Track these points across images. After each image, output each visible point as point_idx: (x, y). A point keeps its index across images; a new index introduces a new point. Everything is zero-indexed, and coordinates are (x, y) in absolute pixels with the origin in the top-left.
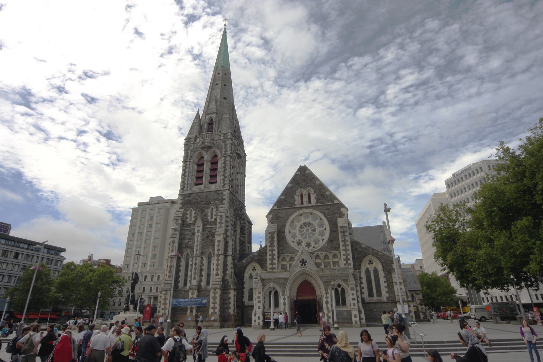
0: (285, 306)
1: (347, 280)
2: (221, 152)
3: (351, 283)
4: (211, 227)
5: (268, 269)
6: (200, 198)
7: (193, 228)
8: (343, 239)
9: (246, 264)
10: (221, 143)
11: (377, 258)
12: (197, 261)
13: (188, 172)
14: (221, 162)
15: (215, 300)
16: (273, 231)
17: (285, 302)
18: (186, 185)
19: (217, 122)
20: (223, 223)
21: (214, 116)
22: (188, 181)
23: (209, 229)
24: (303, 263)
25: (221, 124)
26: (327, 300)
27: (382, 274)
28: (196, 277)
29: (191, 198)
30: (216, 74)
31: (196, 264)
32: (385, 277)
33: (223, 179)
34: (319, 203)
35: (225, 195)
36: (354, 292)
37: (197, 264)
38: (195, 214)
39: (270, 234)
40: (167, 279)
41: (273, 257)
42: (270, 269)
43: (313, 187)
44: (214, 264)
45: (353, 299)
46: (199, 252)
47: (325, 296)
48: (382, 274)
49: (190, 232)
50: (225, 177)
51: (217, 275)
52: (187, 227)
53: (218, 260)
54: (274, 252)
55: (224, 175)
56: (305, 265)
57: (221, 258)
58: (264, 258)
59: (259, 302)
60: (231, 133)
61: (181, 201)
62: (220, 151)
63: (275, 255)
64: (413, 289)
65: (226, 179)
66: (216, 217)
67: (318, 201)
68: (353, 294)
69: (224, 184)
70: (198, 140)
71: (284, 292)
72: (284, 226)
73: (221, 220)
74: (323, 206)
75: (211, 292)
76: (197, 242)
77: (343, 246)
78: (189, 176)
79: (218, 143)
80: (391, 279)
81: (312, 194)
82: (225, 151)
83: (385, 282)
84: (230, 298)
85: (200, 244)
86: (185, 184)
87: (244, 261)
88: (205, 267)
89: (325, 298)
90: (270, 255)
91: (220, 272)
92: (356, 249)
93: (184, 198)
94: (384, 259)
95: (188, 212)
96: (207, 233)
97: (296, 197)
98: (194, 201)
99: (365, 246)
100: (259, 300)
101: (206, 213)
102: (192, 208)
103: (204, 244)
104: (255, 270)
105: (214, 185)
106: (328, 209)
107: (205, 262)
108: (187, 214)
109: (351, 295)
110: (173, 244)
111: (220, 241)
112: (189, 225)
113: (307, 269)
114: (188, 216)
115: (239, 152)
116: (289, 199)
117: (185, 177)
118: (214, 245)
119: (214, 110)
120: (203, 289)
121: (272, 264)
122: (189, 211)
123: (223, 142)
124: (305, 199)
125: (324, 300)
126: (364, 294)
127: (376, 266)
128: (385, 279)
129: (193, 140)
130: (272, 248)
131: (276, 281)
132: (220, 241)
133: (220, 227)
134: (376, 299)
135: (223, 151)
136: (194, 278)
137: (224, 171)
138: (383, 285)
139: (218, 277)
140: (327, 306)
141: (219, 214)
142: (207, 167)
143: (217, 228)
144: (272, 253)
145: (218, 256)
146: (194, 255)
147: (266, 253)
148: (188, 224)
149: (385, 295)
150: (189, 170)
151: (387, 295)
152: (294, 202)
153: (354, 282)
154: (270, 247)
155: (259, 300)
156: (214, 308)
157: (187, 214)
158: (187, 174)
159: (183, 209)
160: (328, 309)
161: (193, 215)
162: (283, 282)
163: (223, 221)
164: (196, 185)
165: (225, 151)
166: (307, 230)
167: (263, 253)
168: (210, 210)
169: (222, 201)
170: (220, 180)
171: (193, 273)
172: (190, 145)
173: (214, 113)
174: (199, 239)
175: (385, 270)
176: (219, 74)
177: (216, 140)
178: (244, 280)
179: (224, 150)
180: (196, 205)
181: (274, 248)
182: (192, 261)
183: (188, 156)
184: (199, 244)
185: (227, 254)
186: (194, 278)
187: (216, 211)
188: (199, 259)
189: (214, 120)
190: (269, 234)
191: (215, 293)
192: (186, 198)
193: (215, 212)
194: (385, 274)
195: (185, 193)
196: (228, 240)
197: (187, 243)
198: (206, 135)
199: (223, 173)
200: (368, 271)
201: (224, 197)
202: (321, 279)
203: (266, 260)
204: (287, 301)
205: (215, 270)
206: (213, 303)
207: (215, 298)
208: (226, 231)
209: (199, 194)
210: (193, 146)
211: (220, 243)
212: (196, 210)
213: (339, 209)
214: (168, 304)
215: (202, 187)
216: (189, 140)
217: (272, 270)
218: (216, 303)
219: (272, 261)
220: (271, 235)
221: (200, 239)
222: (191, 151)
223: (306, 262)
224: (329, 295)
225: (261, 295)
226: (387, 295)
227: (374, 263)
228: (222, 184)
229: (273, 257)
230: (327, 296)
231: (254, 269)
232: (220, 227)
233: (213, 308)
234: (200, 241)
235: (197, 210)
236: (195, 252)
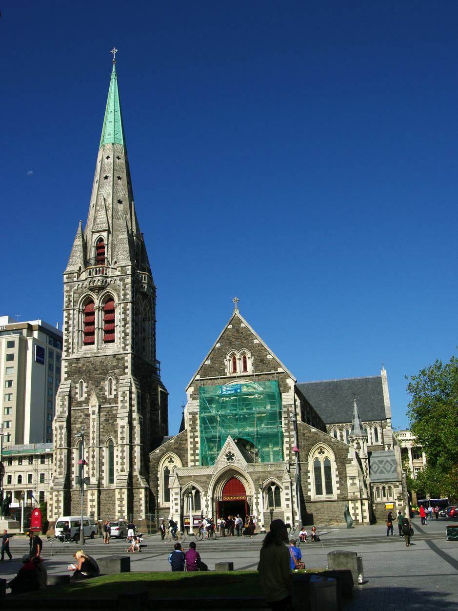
0: (208, 508)
1: (282, 477)
2: (119, 295)
3: (285, 481)
4: (110, 406)
5: (189, 461)
6: (92, 364)
7: (85, 408)
8: (287, 422)
9: (159, 455)
10: (118, 282)
11: (330, 446)
12: (95, 453)
13: (72, 325)
14: (119, 311)
15: (121, 502)
16: (195, 411)
18: (71, 346)
19: (110, 245)
20: (126, 402)
21: (105, 234)
22: (73, 340)
23: (109, 409)
24: (230, 457)
25: (117, 250)
26: (257, 501)
27: (334, 466)
28: (95, 473)
29: (80, 365)
30: (105, 157)
31: (93, 457)
32: (337, 470)
33: (123, 338)
34: (258, 370)
35: (127, 361)
36: (289, 491)
37: (95, 456)
38: (87, 387)
39: (191, 416)
40: (58, 476)
41: (195, 446)
42: (192, 461)
43: (250, 349)
44: (117, 456)
45: (287, 500)
46: (97, 441)
47: (255, 496)
48: (334, 466)
49: (82, 414)
50: (126, 335)
51: (122, 471)
52: (77, 406)
53: (123, 451)
54: (196, 440)
55: (124, 332)
56: (232, 459)
57: (127, 448)
58: (183, 446)
59: (176, 504)
60: (131, 265)
61: (66, 370)
62: (118, 294)
63: (198, 443)
65: (128, 337)
66: (117, 393)
67: (256, 369)
68: (287, 494)
69: (126, 345)
70: (84, 276)
71: (206, 492)
73: (124, 398)
74: (263, 376)
75: (117, 491)
76: (93, 427)
78: (73, 332)
79: (113, 282)
80: (344, 473)
81: (248, 358)
82: (125, 295)
83: (337, 476)
84: (141, 499)
85: (97, 430)
86: (70, 344)
87: (158, 451)
88: (106, 460)
89: (255, 498)
90: (191, 443)
91: (127, 467)
92: (304, 434)
93: (70, 364)
94: (337, 446)
95: (78, 385)
96: (106, 415)
97: (226, 363)
98: (84, 369)
99: (315, 430)
100: (176, 502)
101: (102, 387)
102: (81, 380)
103: (102, 430)
104: (173, 462)
105: (110, 345)
107: (106, 453)
108: (76, 388)
109: (285, 494)
110: (61, 431)
111: (124, 426)
112: (80, 404)
113: (234, 465)
114: (77, 391)
116: (217, 365)
117: (68, 333)
118: (116, 432)
119: (105, 226)
120: (106, 488)
121: (193, 455)
122: (78, 383)
123: (120, 280)
124: (240, 364)
125: (254, 501)
126: (310, 491)
127: (327, 456)
128: (337, 472)
129: (76, 275)
130: (194, 434)
131: (197, 478)
132: (124, 426)
133: (123, 407)
134: (325, 496)
135: (121, 295)
136: (93, 475)
137: (124, 326)
138: (334, 479)
139: (123, 473)
140: (257, 508)
141: (120, 389)
142: (99, 318)
143: (119, 408)
144: (194, 440)
145: (123, 446)
146: (91, 445)
147: (187, 440)
148: (78, 402)
149: (336, 492)
150: (73, 323)
151: (339, 492)
152: (224, 369)
153: (289, 480)
154: (191, 432)
155: (176, 502)
156: (121, 512)
157: (76, 388)
158: (71, 329)
159: (70, 381)
160: (258, 511)
161: (85, 390)
162: (204, 481)
163: (127, 398)
164: (86, 344)
165: (125, 295)
167: (183, 441)
168: (107, 383)
169: (124, 370)
170: (120, 338)
171: (91, 469)
172: (72, 283)
173: (104, 231)
174: (95, 423)
175: (338, 461)
176: (108, 158)
177: (111, 277)
178: (158, 476)
179: (122, 292)
180: (88, 376)
181: (196, 434)
182: (88, 452)
183: (71, 301)
184: (95, 430)
185: (134, 443)
186: (93, 475)
187: (116, 384)
188: (97, 450)
189: (105, 242)
190: (189, 414)
191: (121, 493)
192: (73, 365)
193: (115, 385)
194: (338, 466)
195: (72, 356)
196: (134, 425)
197: (79, 428)
198: (94, 269)
199: (123, 329)
200: (317, 462)
201: (126, 364)
202: (251, 476)
203: (187, 450)
204: (210, 503)
205: (119, 464)
206: (119, 506)
207: (121, 499)
208: (131, 412)
209: (91, 359)
210: (77, 286)
211: (124, 430)
212: (88, 382)
213: (284, 380)
214: (62, 507)
215: (94, 346)
216: (71, 276)
217: (195, 463)
218: (124, 506)
219: (194, 451)
220: (192, 416)
221: (97, 424)
222: (74, 293)
223: (233, 455)
225: (178, 497)
226: (339, 492)
227: (326, 452)
228: (123, 345)
229: (195, 446)
231: (171, 461)
232: (123, 407)
233: (119, 512)
234: (97, 427)
235: (90, 382)
236: (91, 441)
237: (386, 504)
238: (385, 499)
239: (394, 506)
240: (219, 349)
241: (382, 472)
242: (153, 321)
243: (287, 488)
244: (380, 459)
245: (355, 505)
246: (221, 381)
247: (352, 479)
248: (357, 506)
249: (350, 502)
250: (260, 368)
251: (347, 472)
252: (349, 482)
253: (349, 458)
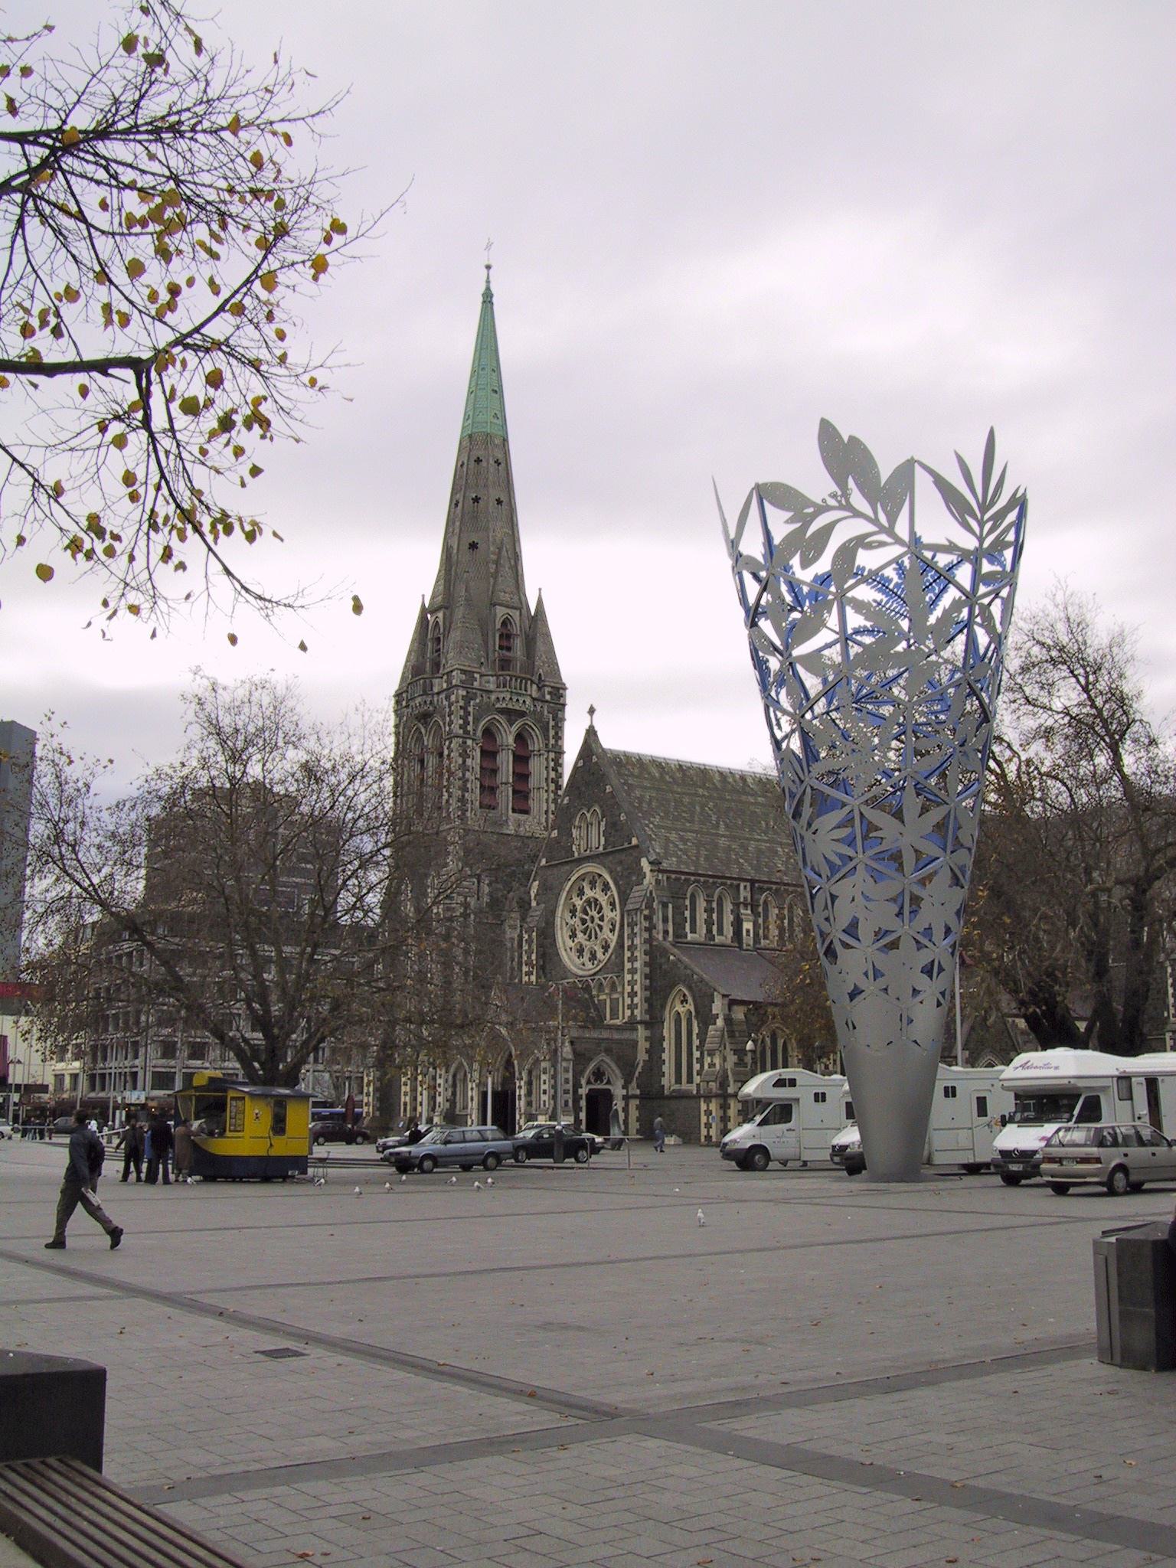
27: (696, 1030)
33: (447, 801)
48: (696, 1030)
50: (450, 796)
72: (553, 912)
77: (629, 960)
106: (621, 862)
115: (504, 705)
165: (450, 726)
166: (592, 918)
240: (568, 806)
242: (552, 755)
246: (567, 867)
249: (702, 1100)
250: (612, 839)
252: (707, 1060)
253: (714, 1012)
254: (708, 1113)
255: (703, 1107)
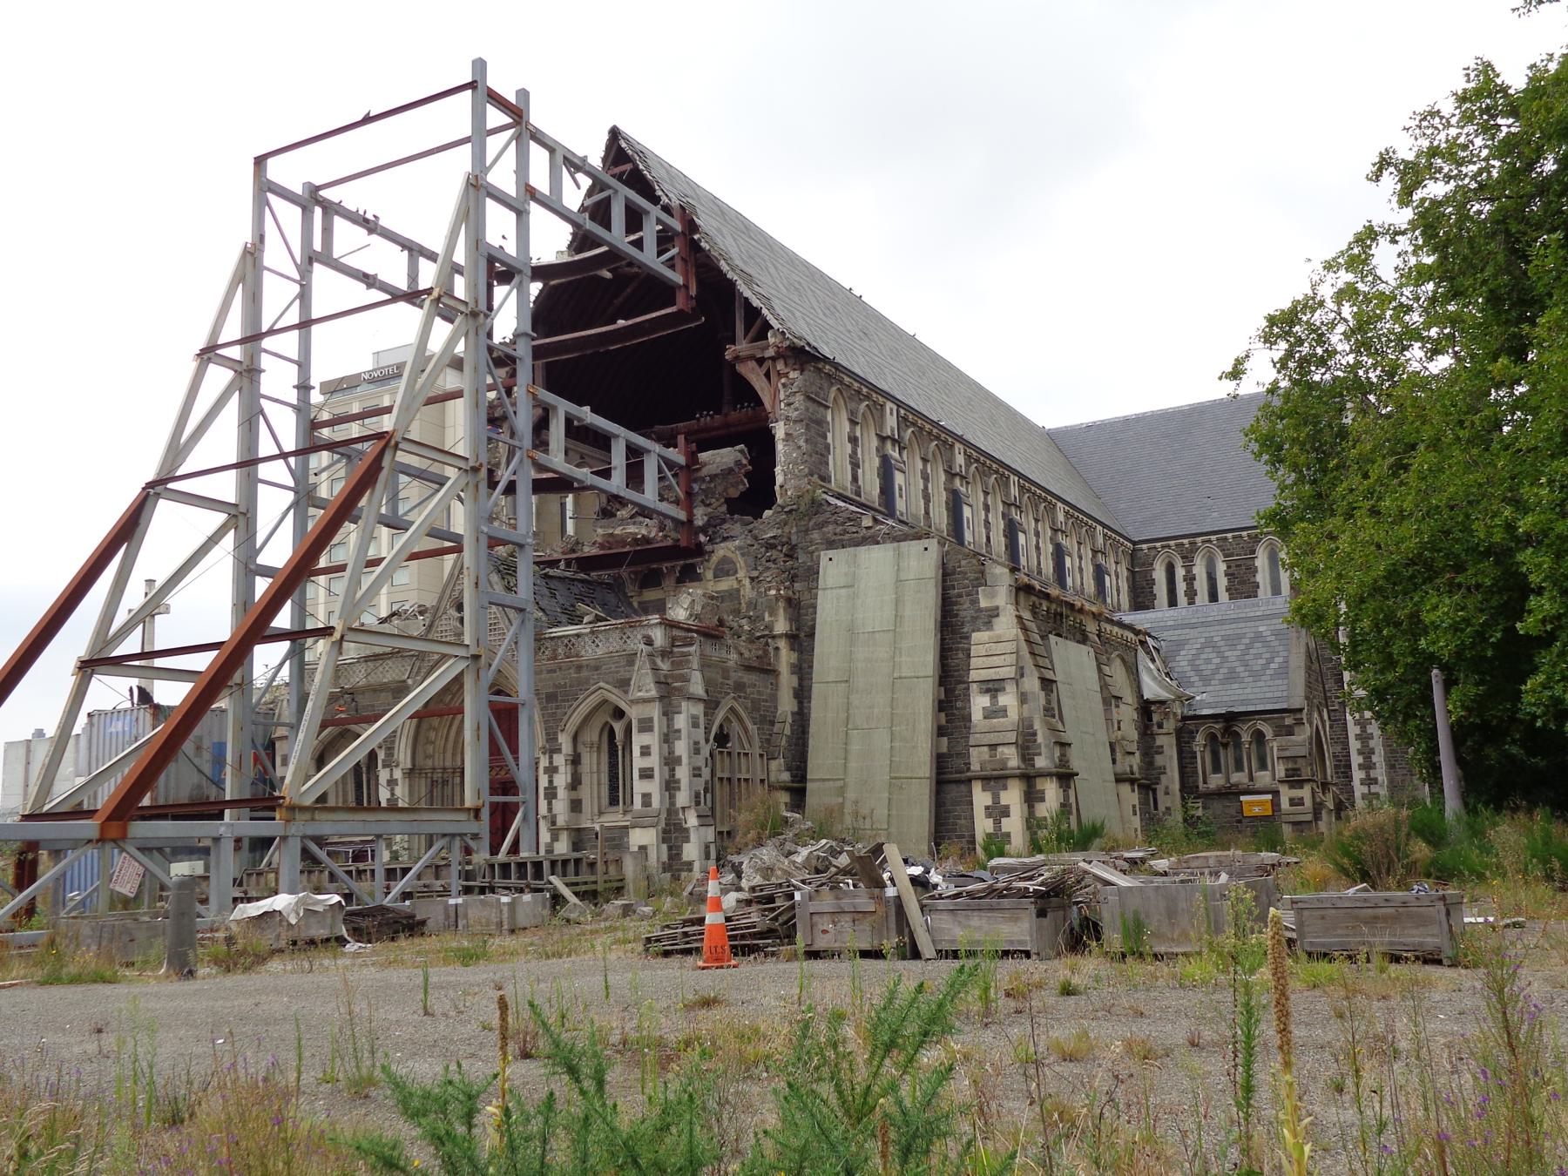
17: (393, 794)
26: (551, 782)
45: (647, 774)
64: (1260, 708)
68: (645, 751)
140: (550, 810)
160: (554, 823)
224: (559, 760)
230: (551, 763)
237: (1242, 798)
238: (1239, 778)
239: (1275, 804)
241: (1232, 677)
243: (646, 726)
244: (1229, 629)
245: (996, 798)
247: (988, 691)
248: (1003, 802)
251: (974, 662)
252: (979, 703)
254: (998, 812)
255: (981, 798)
